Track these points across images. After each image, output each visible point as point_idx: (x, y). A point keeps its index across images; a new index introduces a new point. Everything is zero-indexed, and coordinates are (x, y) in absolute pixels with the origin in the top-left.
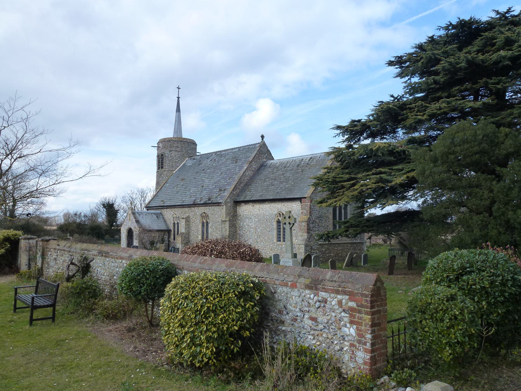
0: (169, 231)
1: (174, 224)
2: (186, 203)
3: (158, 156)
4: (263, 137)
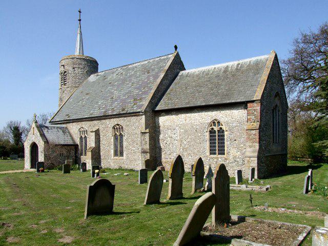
2: (95, 116)
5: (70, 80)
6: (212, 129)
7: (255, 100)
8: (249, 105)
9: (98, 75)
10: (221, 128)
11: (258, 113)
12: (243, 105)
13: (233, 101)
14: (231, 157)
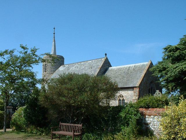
5: (48, 70)
6: (120, 99)
9: (64, 67)
10: (124, 99)
11: (138, 93)
12: (132, 88)
13: (128, 86)
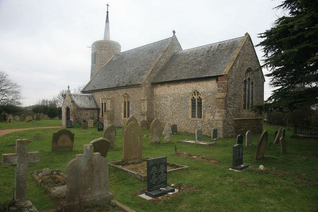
0: (98, 109)
1: (102, 104)
3: (92, 55)
4: (174, 32)
6: (193, 97)
7: (223, 75)
8: (219, 78)
12: (216, 78)
13: (208, 76)
14: (206, 120)
